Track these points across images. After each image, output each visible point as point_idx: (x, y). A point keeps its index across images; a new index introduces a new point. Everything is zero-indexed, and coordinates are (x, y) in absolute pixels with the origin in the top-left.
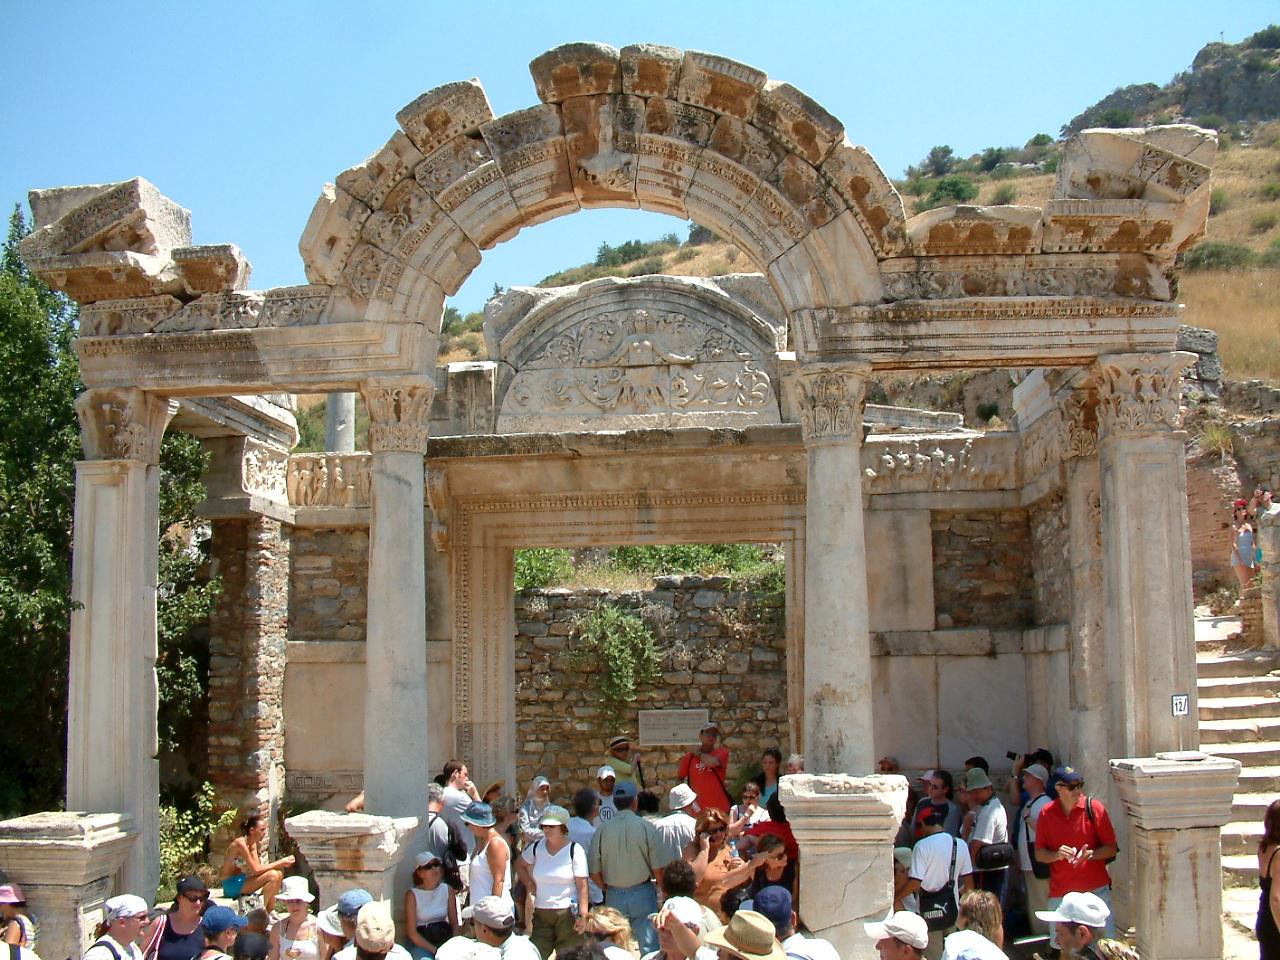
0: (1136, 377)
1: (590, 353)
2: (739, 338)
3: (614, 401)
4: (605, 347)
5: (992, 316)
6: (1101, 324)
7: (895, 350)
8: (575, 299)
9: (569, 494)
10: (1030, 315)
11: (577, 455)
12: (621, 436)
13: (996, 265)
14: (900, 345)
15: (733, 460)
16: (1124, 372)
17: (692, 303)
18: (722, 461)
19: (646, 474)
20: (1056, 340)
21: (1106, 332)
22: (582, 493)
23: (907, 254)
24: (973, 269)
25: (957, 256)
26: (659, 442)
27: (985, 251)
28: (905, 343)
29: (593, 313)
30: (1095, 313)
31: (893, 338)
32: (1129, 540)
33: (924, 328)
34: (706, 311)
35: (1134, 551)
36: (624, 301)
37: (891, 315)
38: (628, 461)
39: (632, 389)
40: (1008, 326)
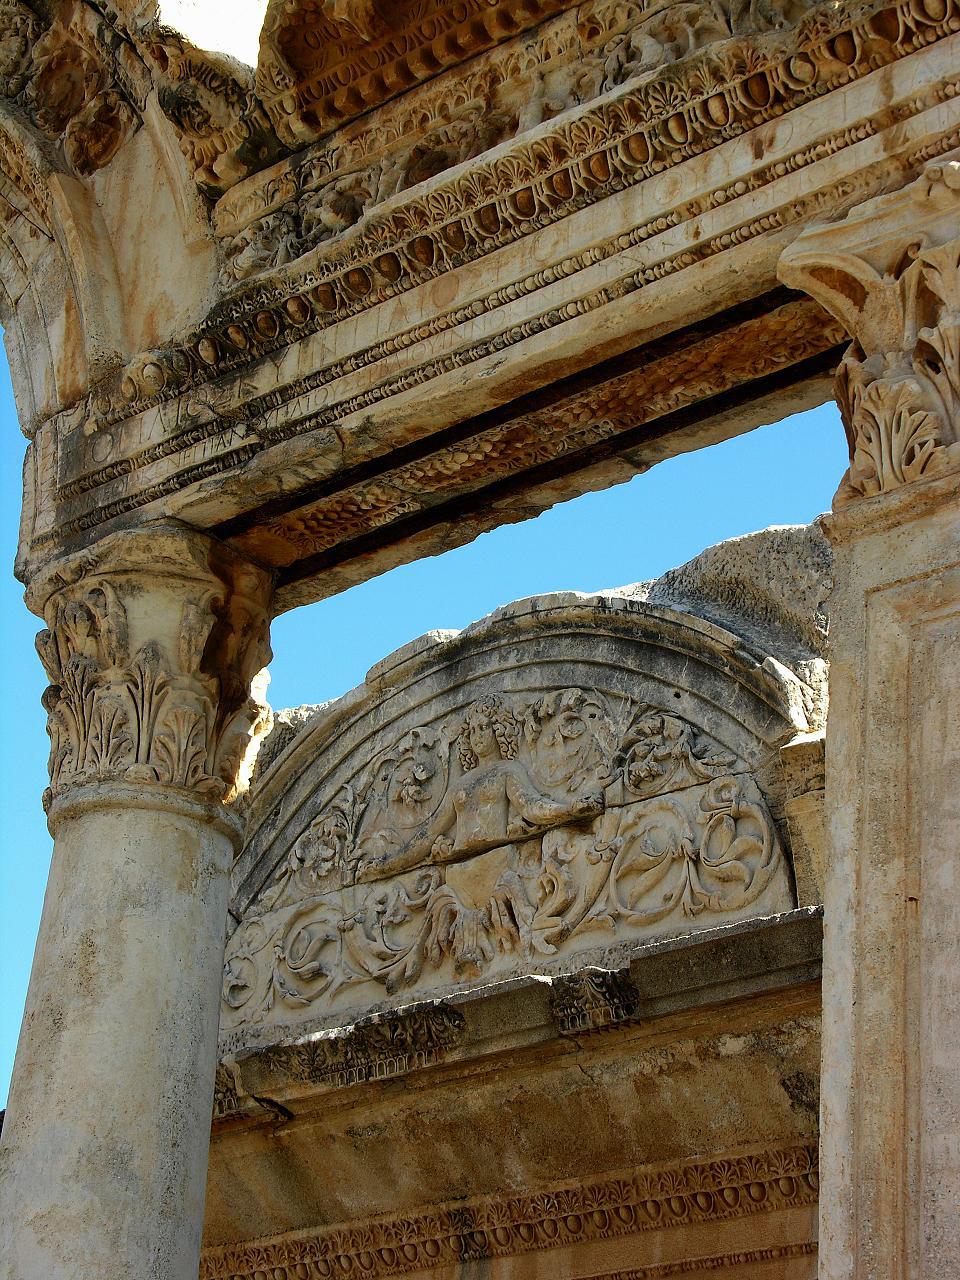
0: (911, 274)
1: (376, 843)
2: (704, 721)
3: (411, 959)
4: (409, 819)
5: (463, 247)
6: (791, 131)
7: (223, 461)
8: (357, 707)
9: (300, 1235)
10: (566, 197)
11: (285, 1114)
12: (348, 1040)
13: (495, 80)
14: (237, 439)
15: (632, 1070)
16: (865, 274)
17: (602, 652)
18: (606, 1078)
19: (446, 1150)
20: (657, 249)
21: (811, 154)
22: (332, 1228)
23: (259, 152)
24: (435, 122)
25: (386, 95)
26: (435, 1045)
27: (453, 46)
28: (250, 429)
29: (390, 736)
30: (767, 98)
31: (224, 424)
32: (859, 956)
33: (294, 364)
34: (630, 664)
35: (878, 1003)
36: (455, 689)
37: (206, 352)
38: (389, 1110)
39: (453, 915)
40: (509, 265)
